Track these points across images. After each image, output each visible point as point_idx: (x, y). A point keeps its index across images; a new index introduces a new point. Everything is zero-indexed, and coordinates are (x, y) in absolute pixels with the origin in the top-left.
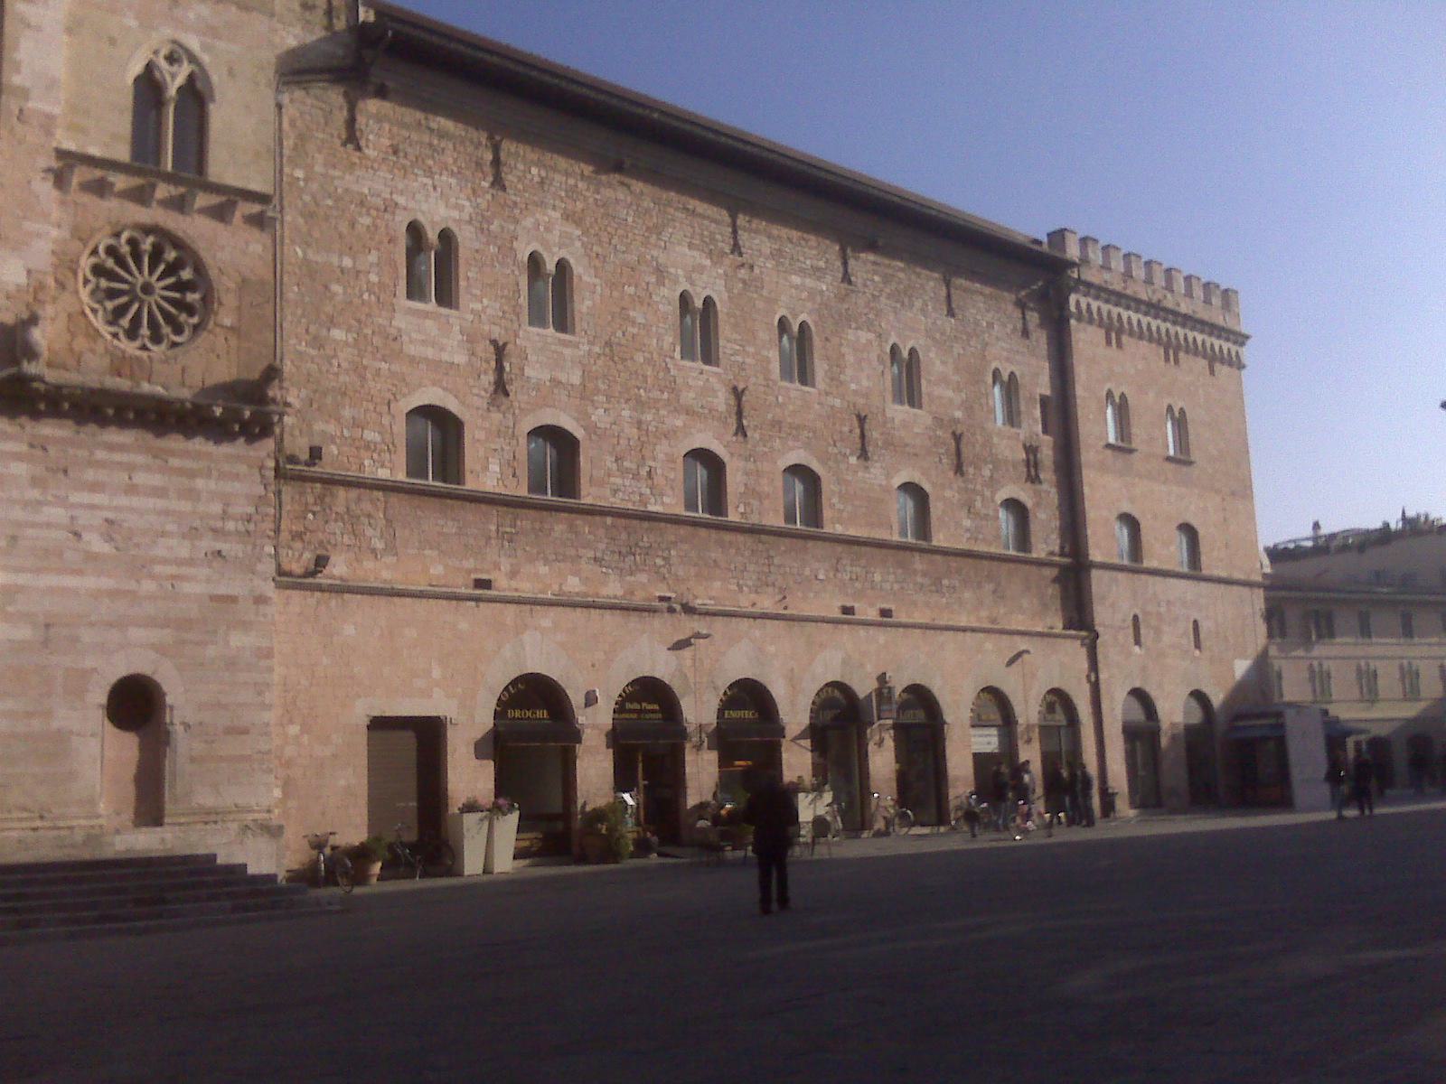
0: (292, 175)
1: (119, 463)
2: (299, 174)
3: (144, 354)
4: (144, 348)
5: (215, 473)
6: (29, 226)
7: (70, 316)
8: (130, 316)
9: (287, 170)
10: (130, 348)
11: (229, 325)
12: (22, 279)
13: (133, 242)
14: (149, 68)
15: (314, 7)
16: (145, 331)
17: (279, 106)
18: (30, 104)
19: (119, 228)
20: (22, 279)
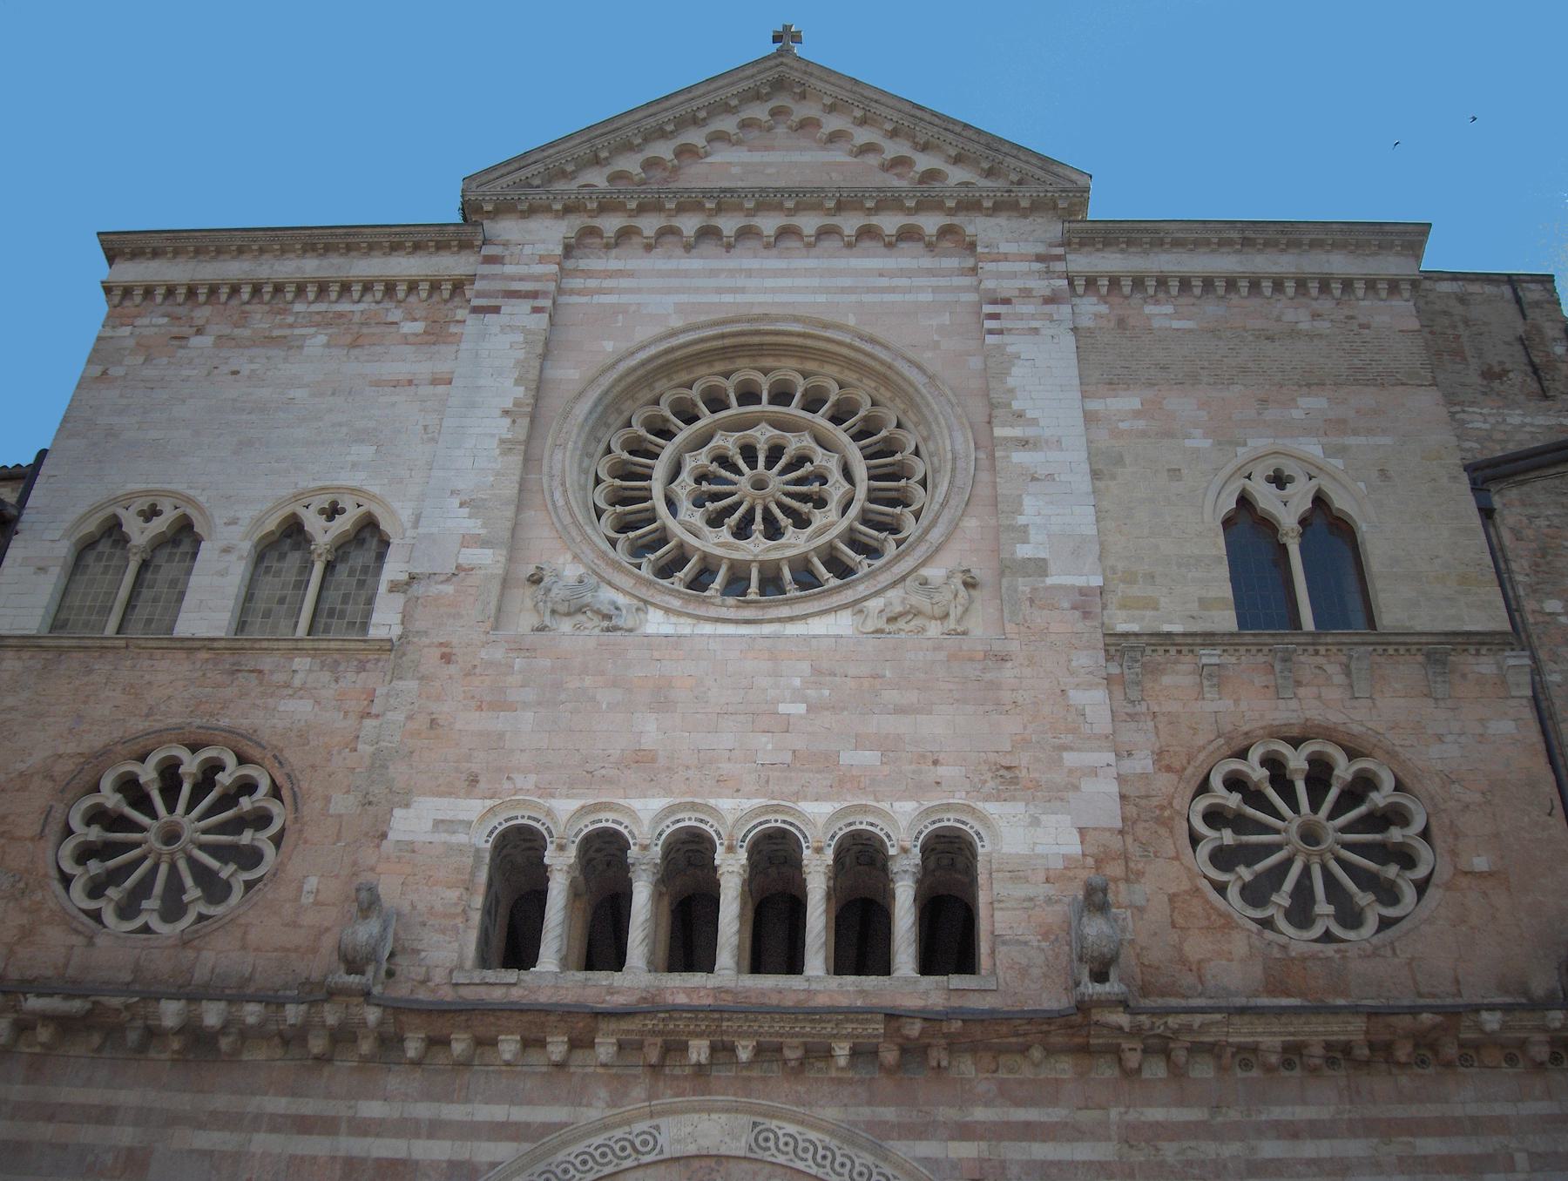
0: (1542, 612)
1: (1311, 1162)
2: (1553, 605)
3: (1329, 949)
4: (1327, 937)
5: (1521, 1159)
6: (1070, 759)
7: (1172, 898)
8: (1289, 885)
9: (1529, 605)
10: (1299, 940)
11: (1485, 867)
12: (1073, 847)
13: (1274, 764)
14: (1244, 501)
15: (1505, 372)
16: (1323, 907)
17: (1487, 513)
18: (1049, 581)
19: (1240, 743)
20: (1073, 847)
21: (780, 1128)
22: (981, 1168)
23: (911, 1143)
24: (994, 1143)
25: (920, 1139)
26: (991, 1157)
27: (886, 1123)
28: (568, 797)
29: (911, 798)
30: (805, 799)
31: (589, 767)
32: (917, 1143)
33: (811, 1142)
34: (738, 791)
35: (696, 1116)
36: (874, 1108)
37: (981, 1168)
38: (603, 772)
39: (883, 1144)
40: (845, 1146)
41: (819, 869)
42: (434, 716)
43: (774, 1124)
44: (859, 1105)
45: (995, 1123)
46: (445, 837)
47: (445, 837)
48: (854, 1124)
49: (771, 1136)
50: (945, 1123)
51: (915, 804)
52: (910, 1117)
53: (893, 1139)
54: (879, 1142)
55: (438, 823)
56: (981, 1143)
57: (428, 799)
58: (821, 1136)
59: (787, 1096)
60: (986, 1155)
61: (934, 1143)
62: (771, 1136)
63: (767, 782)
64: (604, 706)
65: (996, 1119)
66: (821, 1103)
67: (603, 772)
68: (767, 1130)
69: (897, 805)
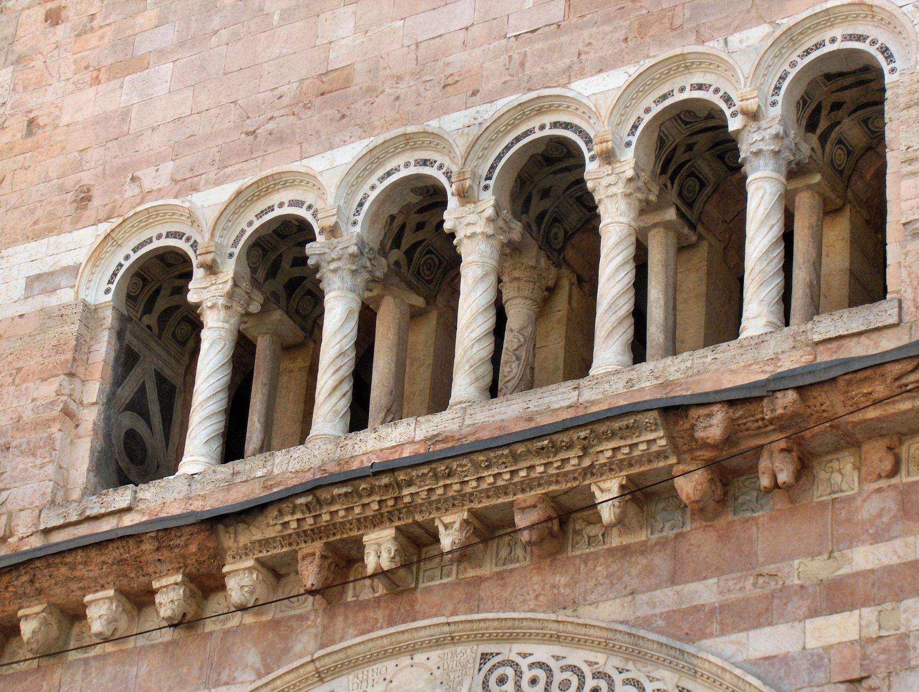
21: (524, 656)
22: (864, 657)
23: (742, 635)
24: (888, 606)
25: (759, 626)
26: (883, 633)
27: (698, 609)
28: (218, 183)
29: (761, 20)
30: (582, 74)
31: (250, 125)
32: (752, 633)
33: (574, 669)
34: (475, 93)
35: (390, 664)
36: (678, 588)
37: (864, 657)
38: (271, 126)
39: (688, 648)
40: (630, 666)
41: (614, 190)
42: (31, 116)
43: (511, 651)
44: (658, 587)
45: (890, 570)
46: (42, 301)
47: (42, 301)
48: (646, 623)
49: (510, 672)
50: (802, 587)
51: (765, 29)
52: (742, 589)
53: (712, 635)
54: (677, 644)
55: (32, 281)
56: (866, 611)
57: (19, 248)
58: (592, 656)
59: (537, 597)
60: (873, 631)
61: (782, 628)
62: (510, 672)
63: (522, 64)
64: (276, 17)
65: (895, 560)
66: (593, 597)
67: (271, 126)
68: (503, 664)
69: (734, 40)
